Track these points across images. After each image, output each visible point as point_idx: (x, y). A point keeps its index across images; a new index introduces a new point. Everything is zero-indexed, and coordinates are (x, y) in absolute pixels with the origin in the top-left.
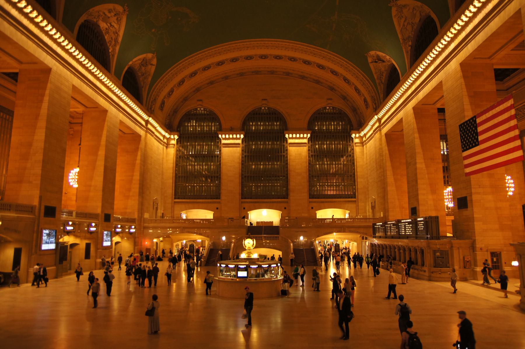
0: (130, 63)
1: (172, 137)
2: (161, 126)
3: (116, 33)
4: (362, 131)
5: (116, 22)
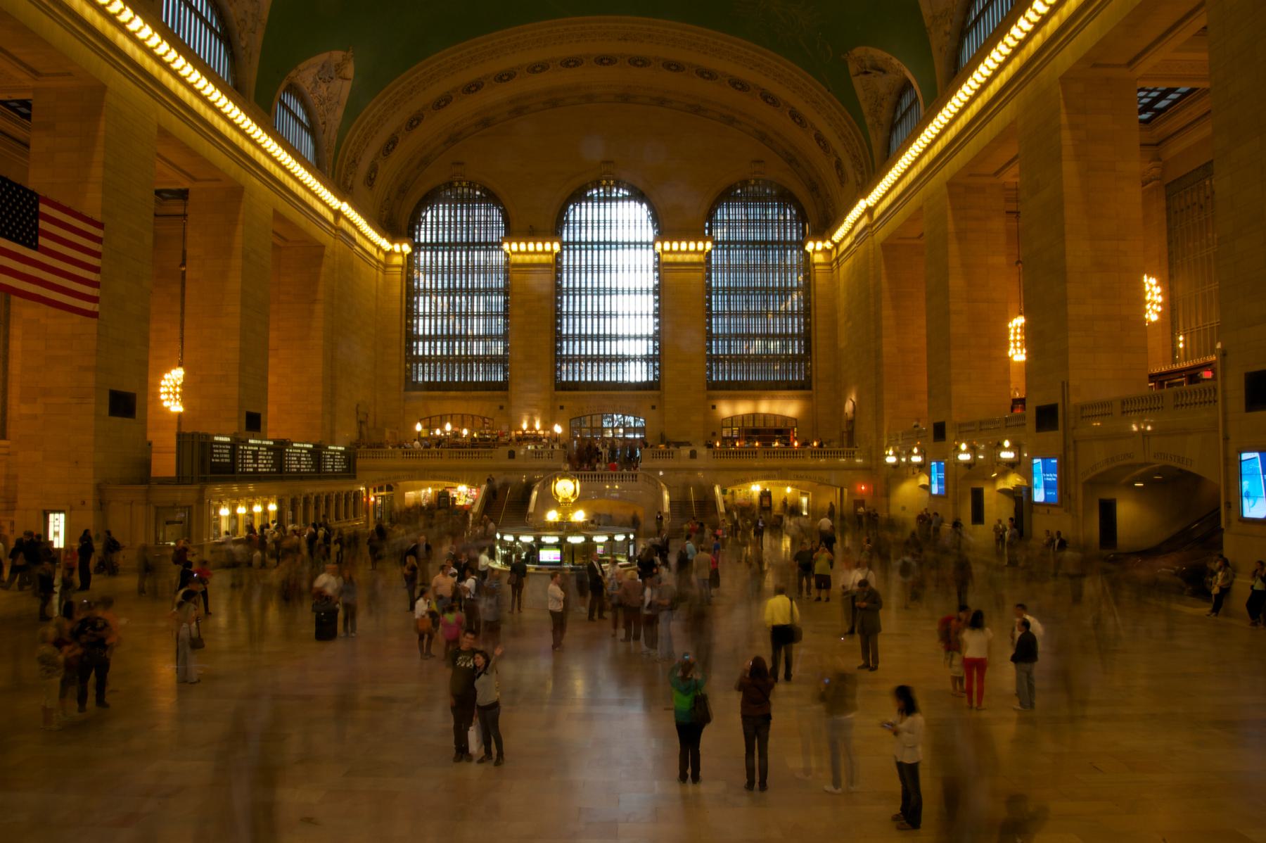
0: (293, 74)
1: (397, 248)
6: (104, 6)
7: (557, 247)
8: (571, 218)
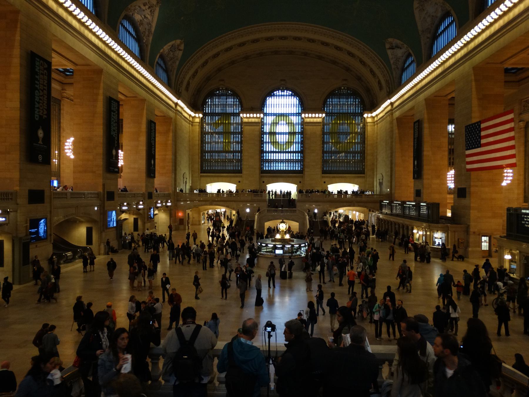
0: (162, 51)
1: (197, 115)
3: (149, 24)
5: (150, 14)
6: (62, 3)
7: (262, 115)
8: (268, 103)
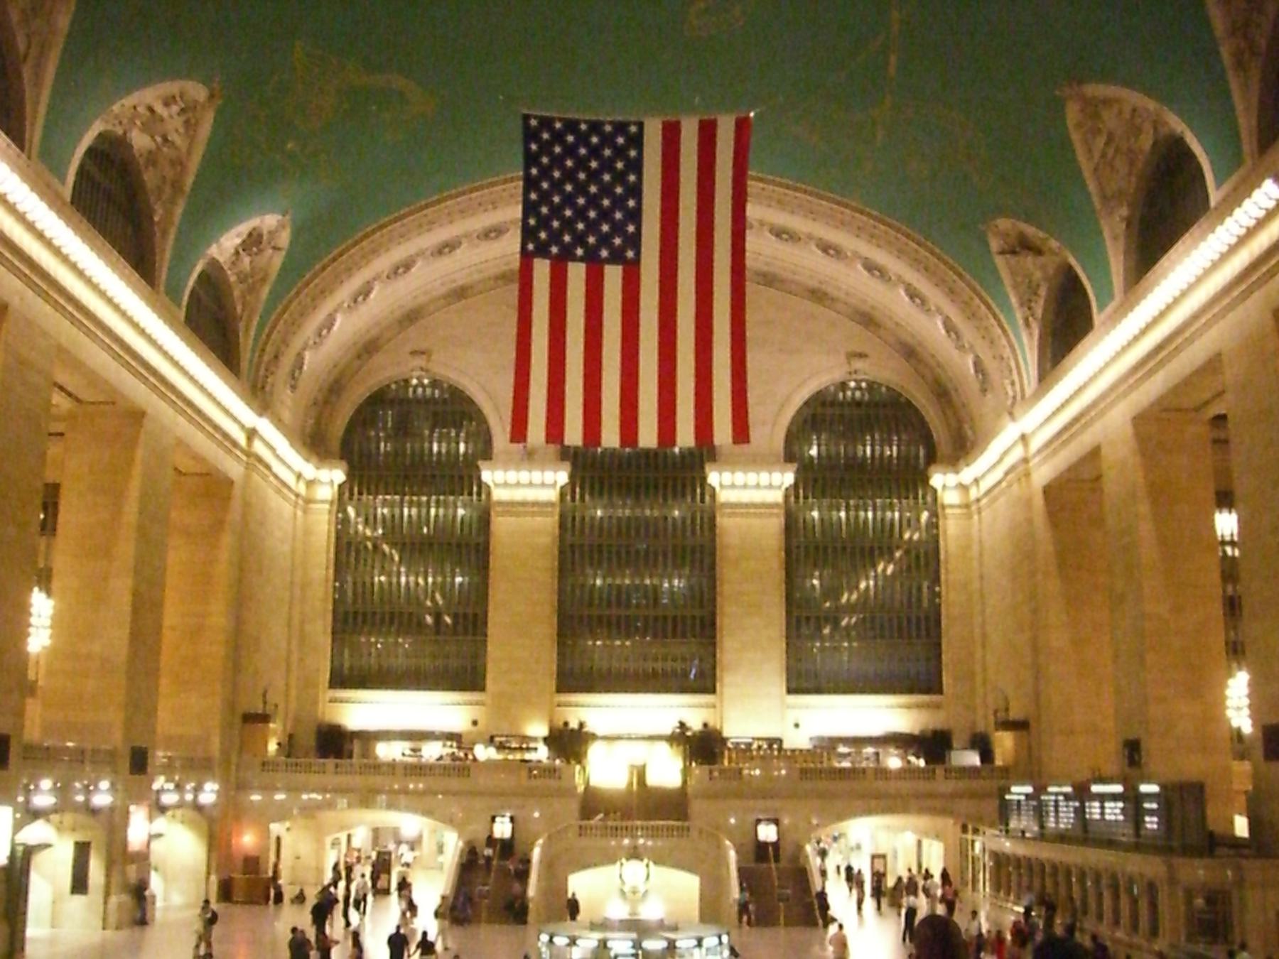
2: (292, 445)
3: (179, 164)
4: (968, 465)
5: (182, 130)
